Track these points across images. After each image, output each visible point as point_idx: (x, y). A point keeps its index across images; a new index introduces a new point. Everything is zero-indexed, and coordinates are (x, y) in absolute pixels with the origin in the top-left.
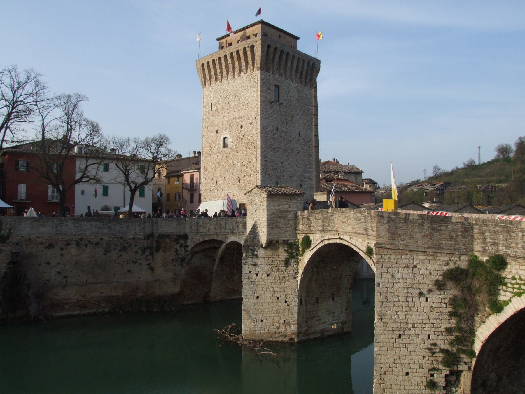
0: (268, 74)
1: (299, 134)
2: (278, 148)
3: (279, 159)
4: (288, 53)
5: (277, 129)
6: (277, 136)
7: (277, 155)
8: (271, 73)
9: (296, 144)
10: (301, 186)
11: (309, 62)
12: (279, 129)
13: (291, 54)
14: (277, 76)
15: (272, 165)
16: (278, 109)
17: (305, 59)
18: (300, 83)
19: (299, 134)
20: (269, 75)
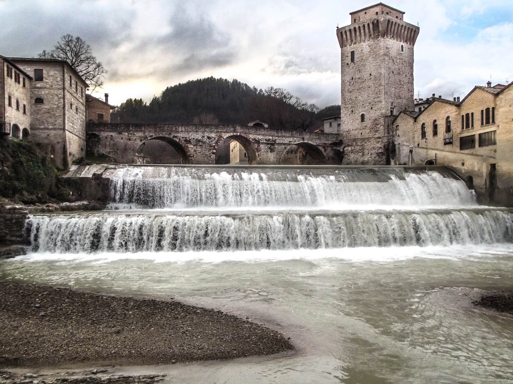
0: (346, 48)
1: (371, 75)
2: (353, 90)
3: (354, 96)
4: (355, 28)
5: (353, 79)
6: (352, 83)
7: (352, 94)
8: (348, 46)
9: (368, 82)
10: (372, 108)
11: (373, 23)
12: (354, 78)
13: (357, 27)
14: (352, 46)
15: (349, 101)
16: (353, 65)
17: (369, 22)
18: (371, 40)
19: (371, 75)
20: (347, 48)
